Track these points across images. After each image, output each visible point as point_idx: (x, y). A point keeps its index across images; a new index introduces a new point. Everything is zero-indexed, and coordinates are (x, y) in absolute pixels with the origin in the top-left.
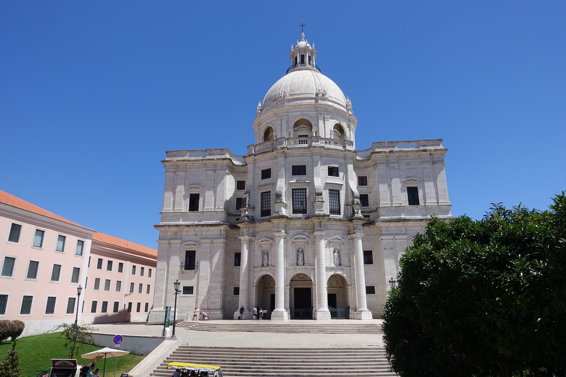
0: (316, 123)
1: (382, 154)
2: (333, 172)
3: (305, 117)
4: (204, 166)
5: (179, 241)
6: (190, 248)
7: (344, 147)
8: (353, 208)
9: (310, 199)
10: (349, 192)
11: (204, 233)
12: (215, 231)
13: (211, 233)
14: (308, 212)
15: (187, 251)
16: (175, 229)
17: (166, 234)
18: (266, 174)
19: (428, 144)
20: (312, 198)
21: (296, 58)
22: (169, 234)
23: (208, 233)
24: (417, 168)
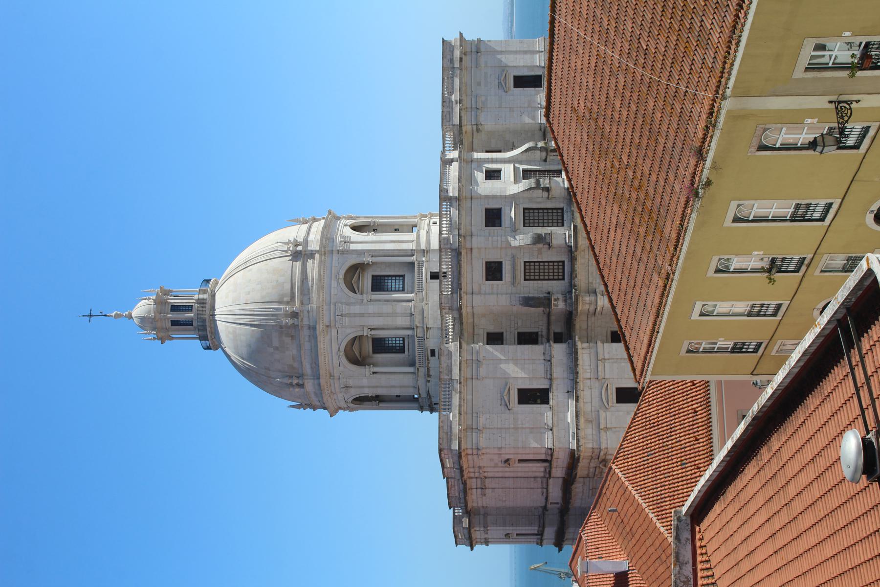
0: (354, 256)
1: (463, 115)
2: (493, 175)
3: (342, 272)
4: (469, 382)
5: (602, 414)
6: (613, 396)
7: (452, 160)
8: (552, 151)
9: (540, 203)
10: (524, 157)
11: (588, 375)
12: (585, 358)
13: (587, 363)
14: (561, 206)
15: (617, 402)
16: (582, 420)
17: (590, 437)
18: (494, 271)
19: (448, 57)
20: (539, 200)
21: (175, 323)
22: (589, 431)
23: (588, 368)
24: (486, 73)
